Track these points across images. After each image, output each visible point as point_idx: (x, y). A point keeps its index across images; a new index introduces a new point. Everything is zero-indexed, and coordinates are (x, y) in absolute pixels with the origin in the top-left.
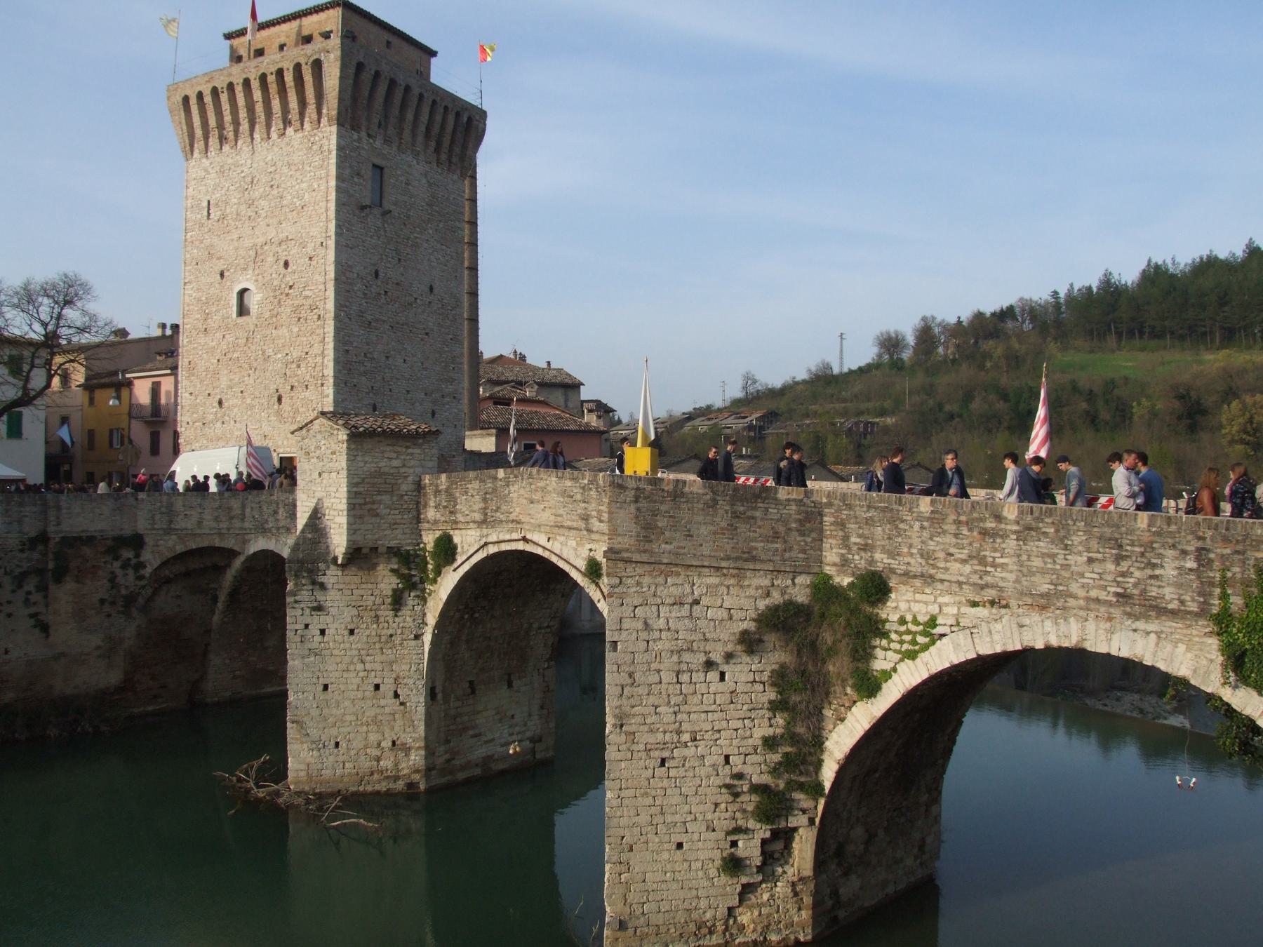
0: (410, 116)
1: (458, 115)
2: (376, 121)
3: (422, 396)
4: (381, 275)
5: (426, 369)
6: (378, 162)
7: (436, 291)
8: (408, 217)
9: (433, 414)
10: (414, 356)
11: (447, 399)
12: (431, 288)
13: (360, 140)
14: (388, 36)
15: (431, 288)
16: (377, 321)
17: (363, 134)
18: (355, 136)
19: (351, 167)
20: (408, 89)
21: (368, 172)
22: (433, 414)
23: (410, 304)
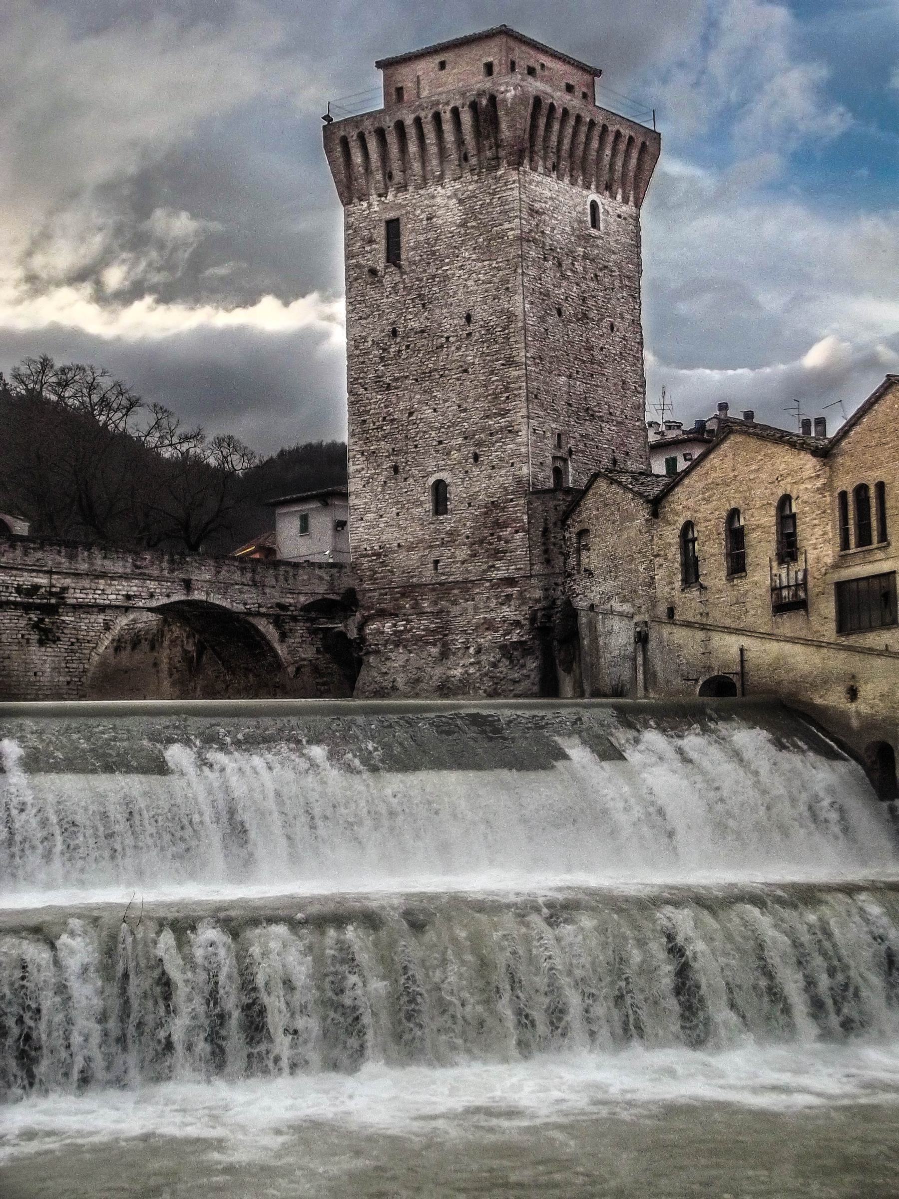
0: (413, 148)
1: (474, 106)
2: (379, 177)
3: (460, 441)
4: (401, 330)
5: (465, 410)
6: (391, 215)
7: (476, 317)
8: (433, 253)
9: (476, 457)
10: (445, 401)
11: (494, 438)
12: (469, 319)
13: (370, 205)
14: (438, 59)
15: (469, 319)
16: (396, 379)
17: (374, 198)
18: (365, 204)
19: (363, 239)
20: (400, 126)
21: (380, 234)
22: (476, 457)
23: (442, 346)
